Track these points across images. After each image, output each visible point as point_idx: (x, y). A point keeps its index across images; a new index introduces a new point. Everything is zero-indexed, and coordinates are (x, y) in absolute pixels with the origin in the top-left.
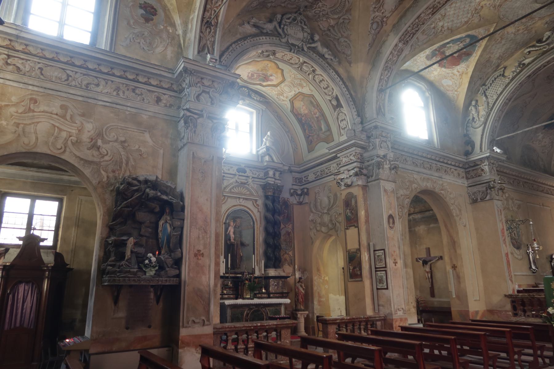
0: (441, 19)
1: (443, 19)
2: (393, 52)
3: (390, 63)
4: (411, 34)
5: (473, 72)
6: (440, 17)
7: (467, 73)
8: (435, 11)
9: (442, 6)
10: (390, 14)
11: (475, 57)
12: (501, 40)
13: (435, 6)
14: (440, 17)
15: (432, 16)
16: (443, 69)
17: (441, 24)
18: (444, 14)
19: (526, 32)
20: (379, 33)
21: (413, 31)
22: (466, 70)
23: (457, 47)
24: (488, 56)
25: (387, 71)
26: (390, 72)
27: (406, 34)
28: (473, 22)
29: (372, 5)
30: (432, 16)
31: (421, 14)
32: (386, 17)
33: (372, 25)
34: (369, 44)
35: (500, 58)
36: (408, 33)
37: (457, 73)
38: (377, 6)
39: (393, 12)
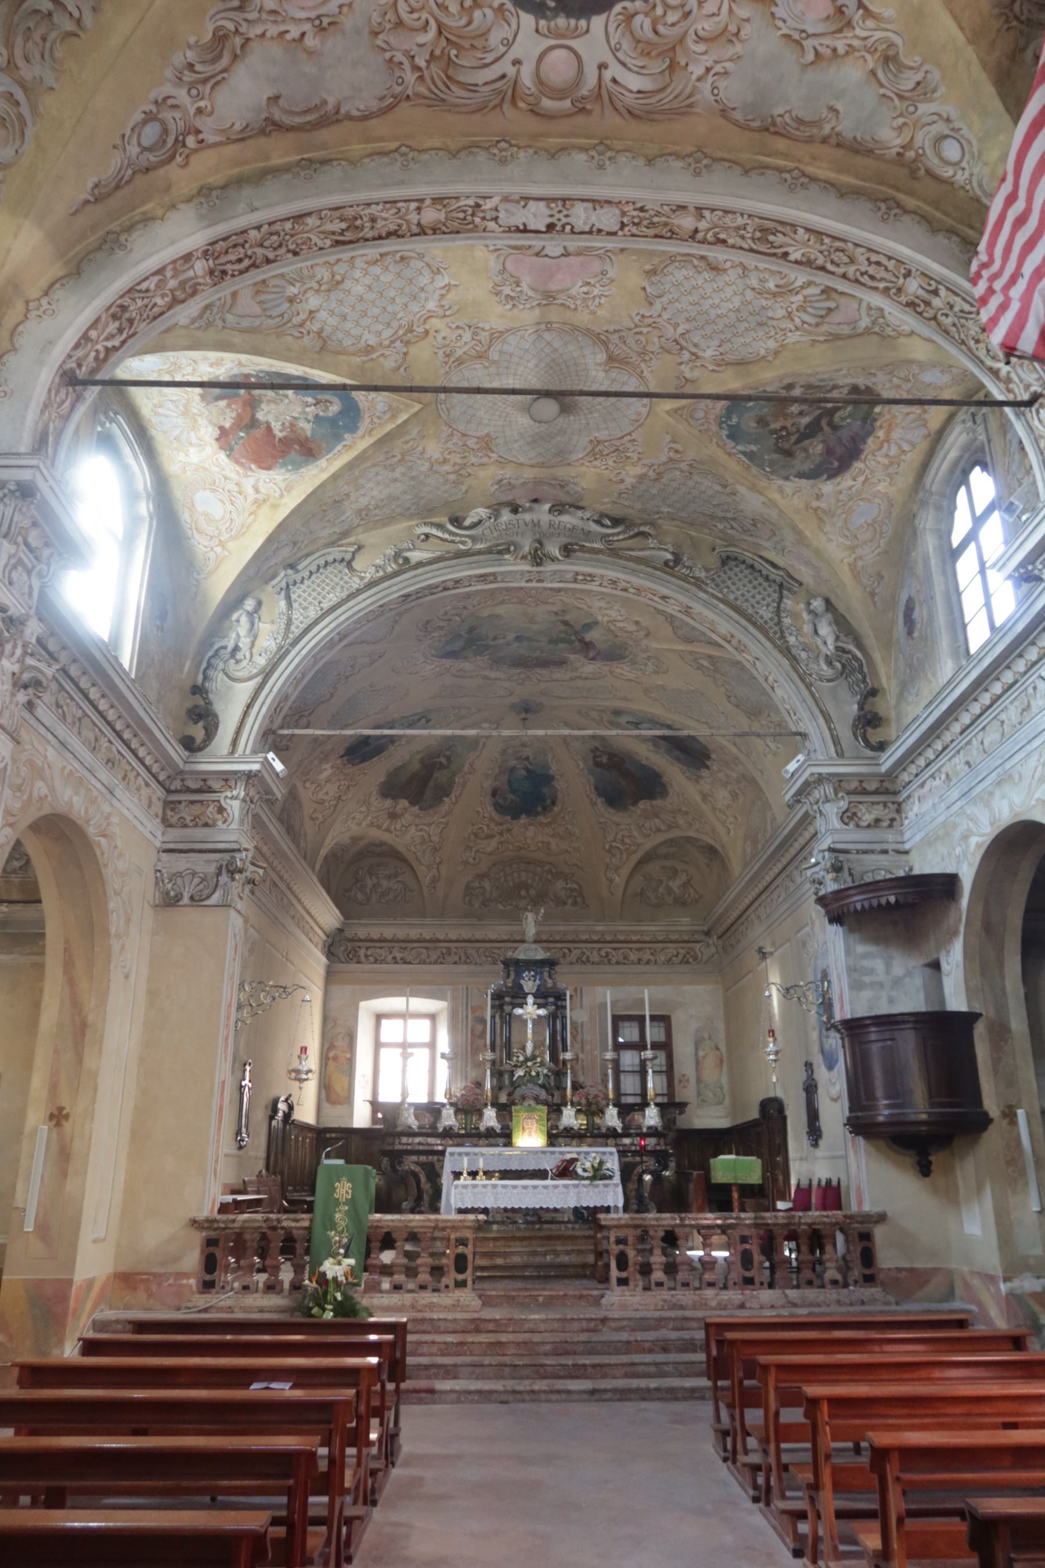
0: (323, 288)
1: (329, 290)
2: (169, 273)
3: (140, 303)
4: (246, 256)
5: (293, 512)
6: (325, 279)
7: (275, 507)
8: (349, 236)
9: (374, 239)
10: (218, 139)
11: (322, 470)
12: (399, 461)
13: (358, 222)
14: (325, 279)
15: (332, 246)
16: (222, 456)
17: (313, 301)
18: (338, 278)
19: (452, 477)
20: (147, 170)
21: (259, 251)
22: (277, 495)
23: (299, 409)
24: (346, 489)
25: (117, 324)
26: (124, 335)
27: (235, 246)
28: (381, 360)
29: (190, 47)
30: (332, 246)
31: (310, 214)
32: (201, 136)
33: (145, 122)
34: (96, 180)
35: (363, 514)
36: (243, 246)
37: (250, 491)
38: (198, 67)
39: (229, 141)
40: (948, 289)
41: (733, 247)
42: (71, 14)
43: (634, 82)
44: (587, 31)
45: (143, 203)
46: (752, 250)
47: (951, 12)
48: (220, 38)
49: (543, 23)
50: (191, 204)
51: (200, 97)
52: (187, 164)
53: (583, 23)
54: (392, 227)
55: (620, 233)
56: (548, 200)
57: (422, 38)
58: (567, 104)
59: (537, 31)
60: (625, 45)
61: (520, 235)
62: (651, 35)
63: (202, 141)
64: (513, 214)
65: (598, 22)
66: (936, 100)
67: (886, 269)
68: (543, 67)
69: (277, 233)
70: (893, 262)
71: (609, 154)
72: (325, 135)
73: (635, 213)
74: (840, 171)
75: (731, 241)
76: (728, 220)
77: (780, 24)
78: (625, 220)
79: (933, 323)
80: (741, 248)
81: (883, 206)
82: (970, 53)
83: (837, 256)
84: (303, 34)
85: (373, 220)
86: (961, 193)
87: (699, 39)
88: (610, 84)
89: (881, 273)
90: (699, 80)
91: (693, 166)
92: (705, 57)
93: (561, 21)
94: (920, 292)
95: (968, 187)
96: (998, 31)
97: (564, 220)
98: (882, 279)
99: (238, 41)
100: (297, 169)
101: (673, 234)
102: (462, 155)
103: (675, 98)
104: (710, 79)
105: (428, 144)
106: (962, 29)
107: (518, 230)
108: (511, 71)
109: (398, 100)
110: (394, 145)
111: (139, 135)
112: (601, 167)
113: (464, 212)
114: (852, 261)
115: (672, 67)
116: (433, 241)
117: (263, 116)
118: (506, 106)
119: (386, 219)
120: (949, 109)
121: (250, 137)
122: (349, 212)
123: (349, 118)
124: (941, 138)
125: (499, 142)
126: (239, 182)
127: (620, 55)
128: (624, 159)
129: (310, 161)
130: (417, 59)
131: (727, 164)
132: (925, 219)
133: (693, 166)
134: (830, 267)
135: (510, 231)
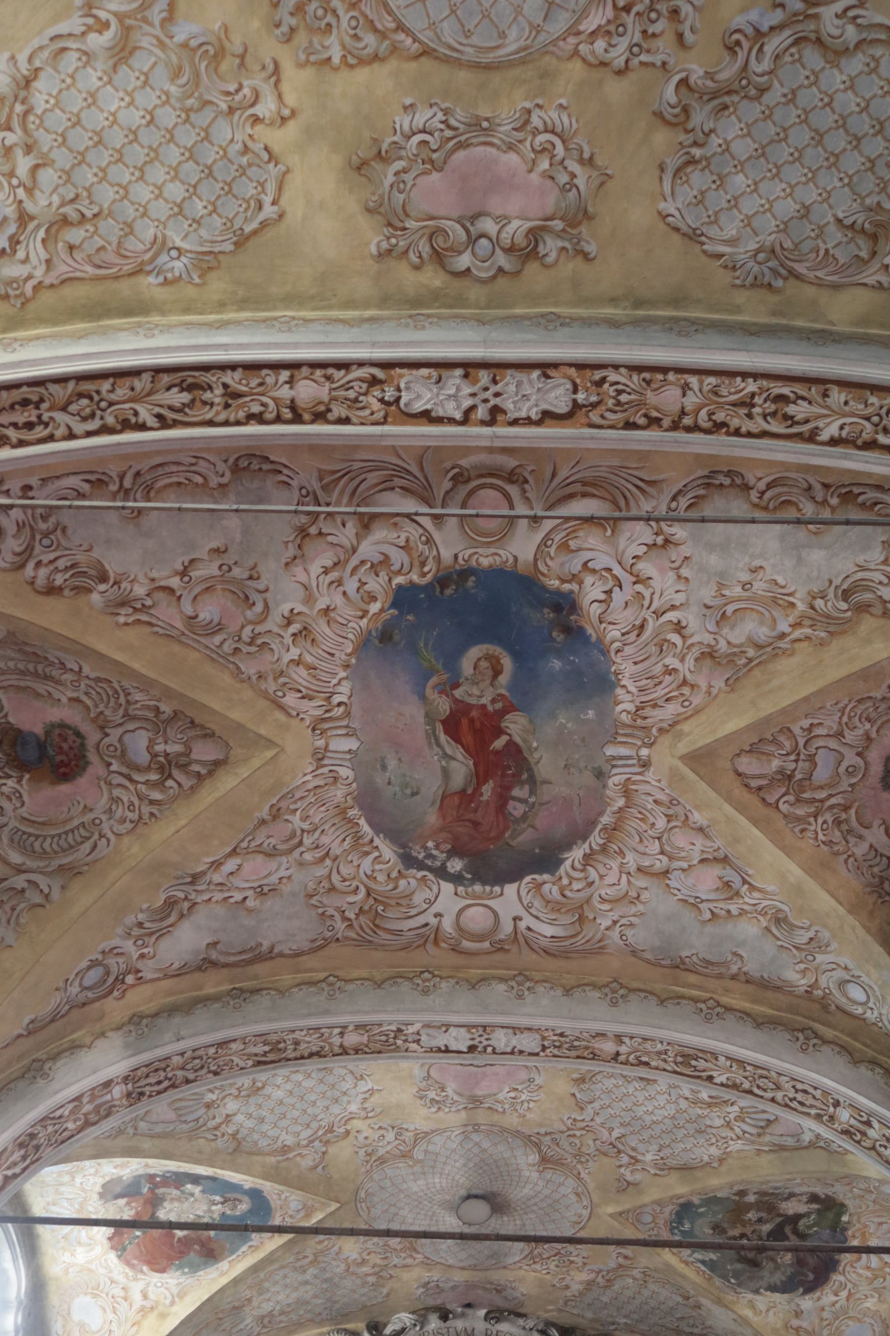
0: (242, 1094)
1: (249, 1096)
2: (85, 1100)
3: (50, 1129)
4: (166, 1078)
5: (183, 1323)
6: (246, 1085)
7: (163, 1316)
8: (271, 1057)
9: (296, 1059)
10: (156, 976)
11: (222, 1274)
12: (311, 1262)
13: (282, 1045)
14: (246, 1085)
15: (254, 1066)
16: (112, 1256)
17: (231, 1106)
18: (259, 1084)
19: (372, 1279)
20: (84, 1004)
21: (180, 1073)
22: (168, 1302)
23: (205, 1208)
24: (248, 1294)
25: (22, 1152)
26: (28, 1161)
27: (156, 1070)
28: (298, 1159)
29: (142, 911)
30: (254, 1066)
31: (234, 1040)
32: (140, 975)
33: (89, 968)
34: (33, 1016)
35: (266, 1321)
36: (164, 1070)
37: (137, 1297)
38: (147, 925)
39: (166, 977)
40: (880, 1122)
41: (657, 1068)
42: (41, 891)
43: (548, 930)
44: (502, 894)
45: (74, 1031)
46: (675, 1072)
47: (828, 891)
48: (170, 904)
49: (460, 889)
50: (120, 1032)
51: (145, 946)
52: (123, 997)
53: (497, 889)
54: (315, 1049)
55: (542, 1054)
56: (469, 1027)
57: (352, 899)
58: (486, 945)
59: (456, 894)
60: (536, 904)
61: (441, 1055)
62: (560, 898)
63: (141, 978)
64: (435, 1038)
65: (510, 889)
66: (831, 952)
67: (814, 1097)
68: (462, 918)
69: (201, 1058)
70: (819, 1092)
71: (528, 984)
72: (259, 969)
73: (556, 1038)
74: (754, 1001)
75: (653, 1064)
76: (648, 1045)
77: (676, 892)
78: (546, 1043)
79: (873, 1153)
80: (665, 1070)
81: (801, 1036)
82: (851, 920)
83: (762, 1082)
84: (245, 898)
85: (297, 1043)
86: (875, 1028)
87: (603, 900)
88: (525, 931)
89: (810, 1101)
90: (607, 929)
91: (610, 996)
92: (611, 914)
93: (478, 888)
94: (853, 1122)
95: (880, 1024)
96: (874, 904)
97: (485, 1043)
98: (811, 1106)
99: (186, 905)
100: (228, 998)
101: (594, 1056)
102: (386, 985)
103: (588, 941)
104: (617, 929)
105: (356, 974)
106: (841, 904)
107: (439, 1050)
108: (434, 921)
109: (327, 942)
110: (322, 975)
111: (82, 979)
112: (520, 997)
113: (387, 1035)
114: (778, 1087)
115: (582, 919)
116: (354, 1060)
117: (201, 957)
118: (429, 946)
119: (309, 1042)
120: (843, 960)
121: (186, 973)
122: (274, 1038)
123: (281, 955)
124: (842, 983)
125: (422, 972)
126: (172, 1010)
127: (532, 911)
128: (542, 989)
129: (242, 990)
130: (347, 914)
131: (643, 995)
132: (844, 1049)
133: (610, 996)
134: (756, 1091)
135: (431, 1051)
